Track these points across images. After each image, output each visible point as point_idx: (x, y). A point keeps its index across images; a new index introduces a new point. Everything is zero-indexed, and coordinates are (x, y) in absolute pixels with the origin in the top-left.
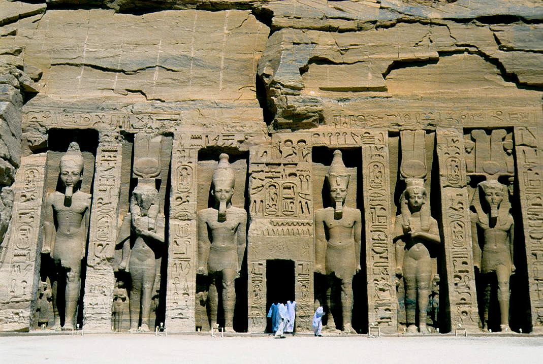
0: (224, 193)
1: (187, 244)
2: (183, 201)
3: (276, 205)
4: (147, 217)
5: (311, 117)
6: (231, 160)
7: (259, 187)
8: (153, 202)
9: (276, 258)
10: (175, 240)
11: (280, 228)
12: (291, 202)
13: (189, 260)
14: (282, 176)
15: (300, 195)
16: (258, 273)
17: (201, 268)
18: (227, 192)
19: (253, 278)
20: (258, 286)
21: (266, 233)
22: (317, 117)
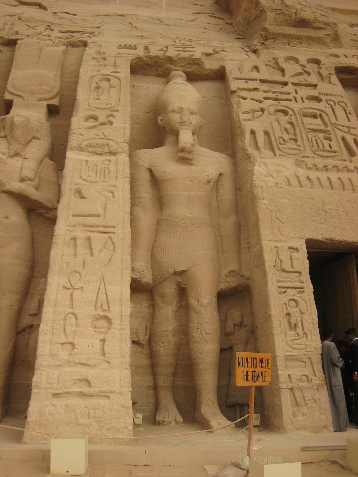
0: (186, 113)
1: (106, 197)
2: (100, 121)
3: (296, 140)
4: (20, 159)
5: (321, 28)
6: (191, 78)
7: (255, 111)
8: (37, 135)
9: (328, 236)
10: (76, 187)
11: (323, 176)
12: (326, 138)
13: (111, 230)
14: (295, 98)
15: (339, 127)
16: (291, 270)
17: (137, 265)
18: (192, 113)
19: (280, 281)
20: (293, 303)
21: (294, 181)
22: (330, 32)
